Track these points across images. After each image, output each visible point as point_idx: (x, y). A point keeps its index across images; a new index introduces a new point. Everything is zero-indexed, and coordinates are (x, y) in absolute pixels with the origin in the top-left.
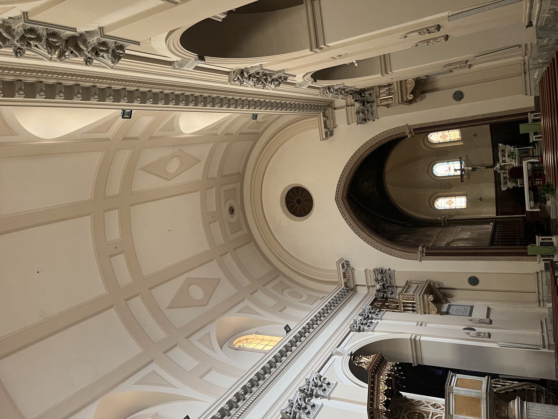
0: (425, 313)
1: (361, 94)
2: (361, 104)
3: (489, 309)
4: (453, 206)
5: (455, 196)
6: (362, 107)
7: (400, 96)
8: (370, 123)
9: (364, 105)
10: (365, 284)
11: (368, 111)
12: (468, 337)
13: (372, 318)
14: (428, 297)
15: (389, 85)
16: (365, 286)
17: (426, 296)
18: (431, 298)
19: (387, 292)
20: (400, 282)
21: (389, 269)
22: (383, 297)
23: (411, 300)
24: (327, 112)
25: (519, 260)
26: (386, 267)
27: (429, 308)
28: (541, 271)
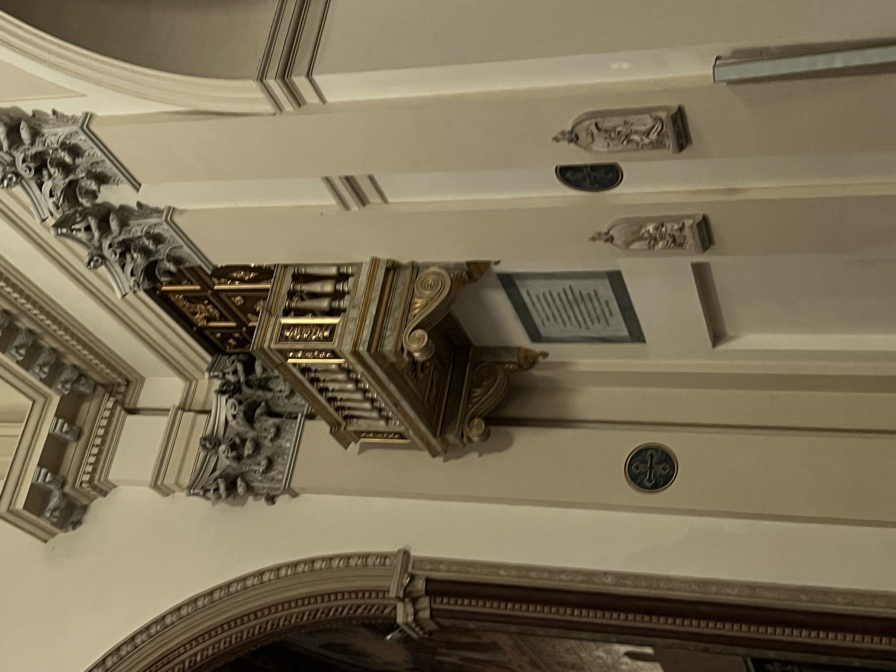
9: (250, 418)
11: (257, 446)
15: (342, 277)
24: (88, 409)
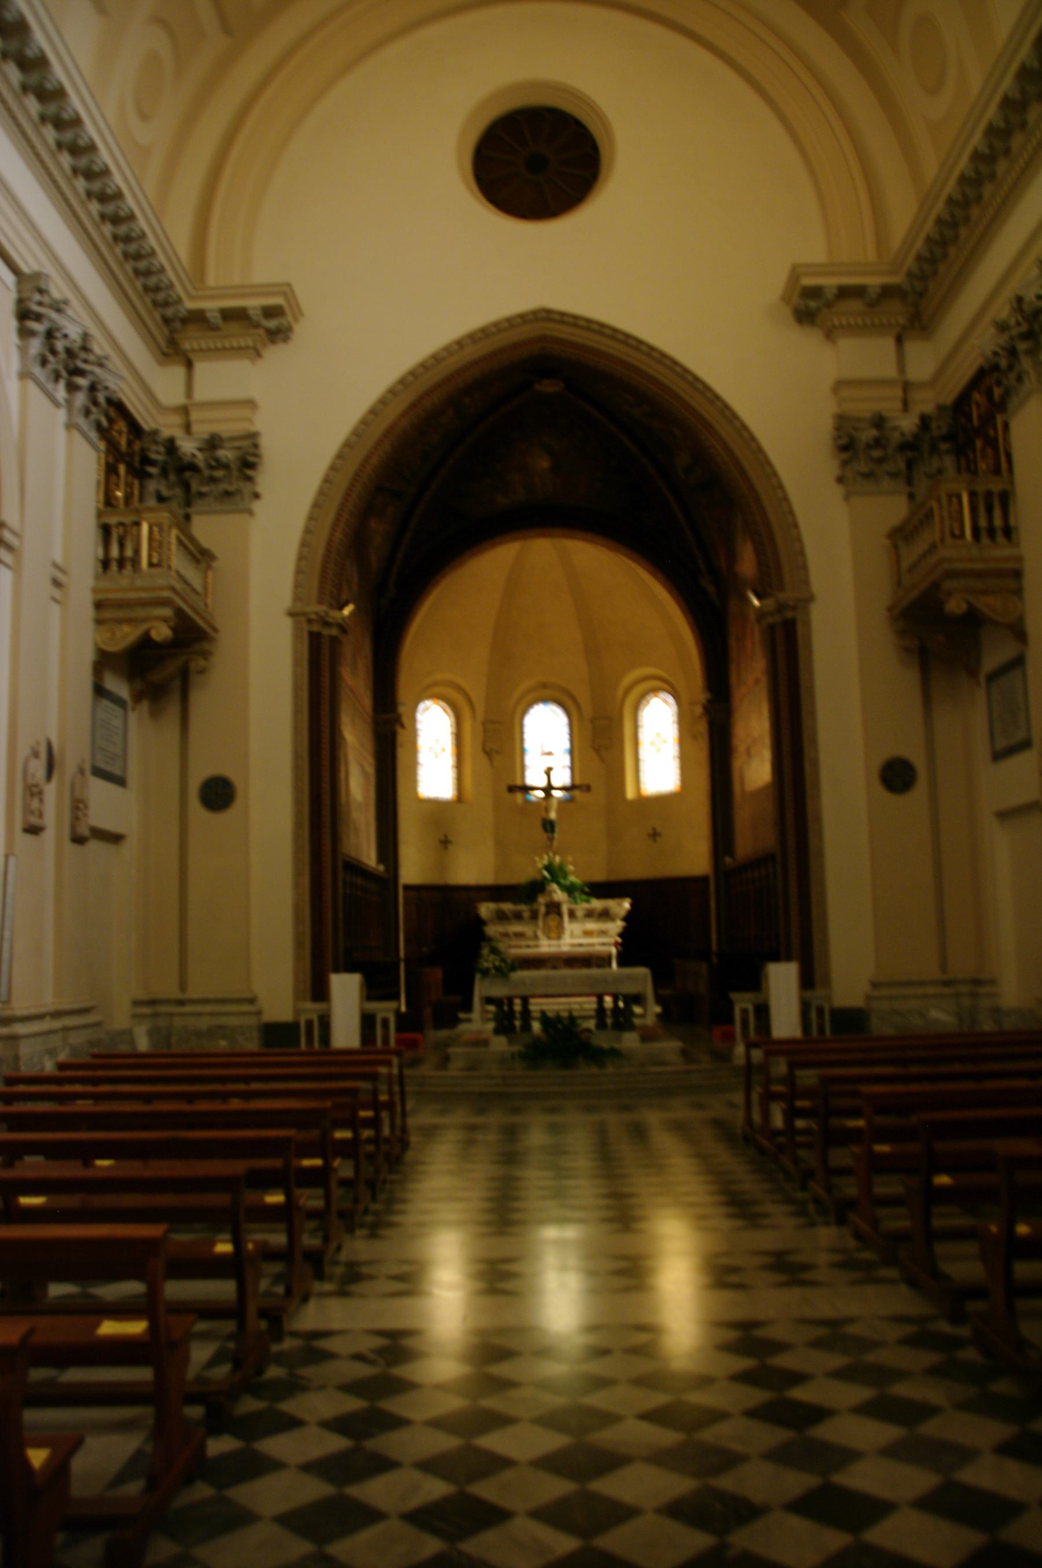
0: (99, 605)
1: (945, 438)
3: (115, 838)
5: (459, 765)
6: (896, 438)
7: (967, 565)
8: (828, 466)
9: (905, 447)
10: (200, 394)
11: (880, 461)
12: (23, 751)
13: (72, 388)
14: (165, 620)
15: (1008, 532)
17: (167, 612)
18: (162, 632)
21: (257, 496)
22: (146, 461)
23: (150, 556)
25: (298, 944)
27: (119, 622)
28: (259, 1013)
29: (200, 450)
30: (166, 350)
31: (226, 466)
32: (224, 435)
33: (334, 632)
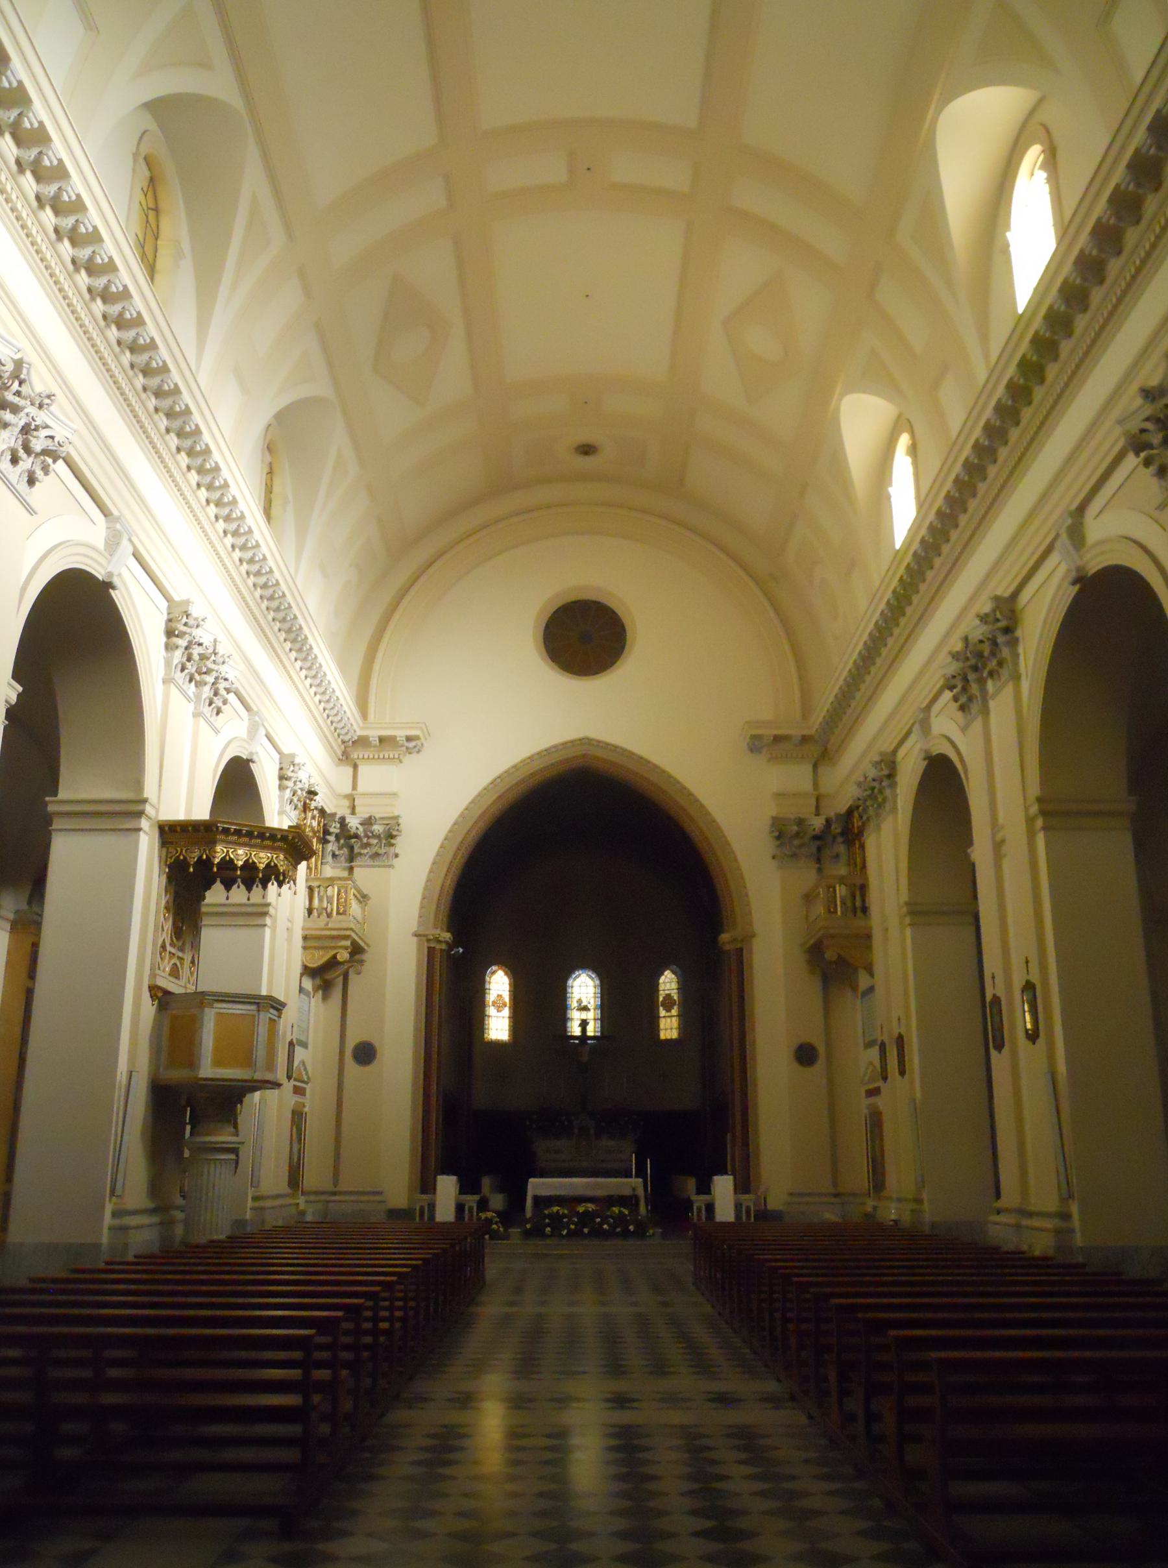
0: (305, 938)
2: (817, 832)
4: (491, 1011)
6: (811, 833)
9: (816, 838)
10: (361, 788)
11: (801, 846)
16: (354, 787)
18: (343, 956)
19: (336, 844)
20: (365, 875)
21: (397, 856)
23: (338, 908)
26: (401, 844)
29: (361, 824)
30: (341, 757)
31: (378, 837)
32: (377, 816)
33: (444, 946)
